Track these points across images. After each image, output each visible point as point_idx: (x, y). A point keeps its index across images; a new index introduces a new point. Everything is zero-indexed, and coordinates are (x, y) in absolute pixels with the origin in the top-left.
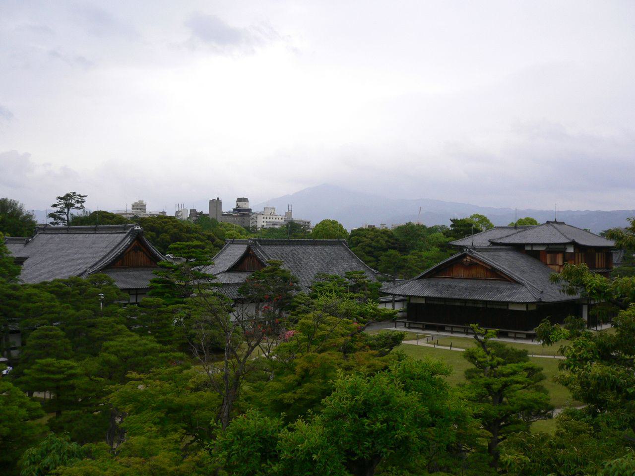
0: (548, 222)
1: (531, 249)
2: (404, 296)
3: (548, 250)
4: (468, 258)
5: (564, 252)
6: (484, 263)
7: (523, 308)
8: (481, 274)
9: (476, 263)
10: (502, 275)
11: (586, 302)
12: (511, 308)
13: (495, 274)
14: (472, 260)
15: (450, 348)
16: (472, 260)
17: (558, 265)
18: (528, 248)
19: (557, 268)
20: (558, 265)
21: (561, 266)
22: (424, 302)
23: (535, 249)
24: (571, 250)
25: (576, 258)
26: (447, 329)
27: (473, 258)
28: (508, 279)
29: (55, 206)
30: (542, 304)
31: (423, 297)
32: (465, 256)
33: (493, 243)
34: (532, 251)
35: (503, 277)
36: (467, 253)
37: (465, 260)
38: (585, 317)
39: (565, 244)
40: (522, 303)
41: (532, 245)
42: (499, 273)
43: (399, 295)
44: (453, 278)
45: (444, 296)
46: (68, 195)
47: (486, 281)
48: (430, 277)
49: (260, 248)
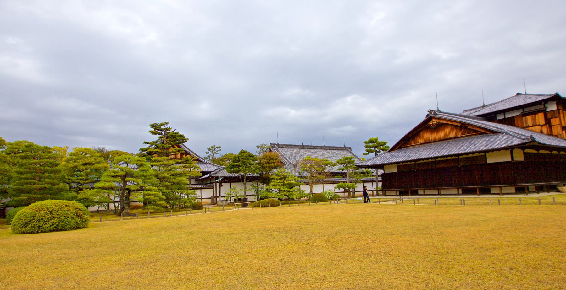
0: (518, 94)
1: (503, 117)
4: (434, 120)
5: (544, 111)
6: (452, 121)
7: (507, 158)
8: (449, 133)
9: (443, 124)
12: (490, 161)
14: (438, 121)
16: (438, 121)
17: (539, 125)
19: (538, 128)
20: (539, 125)
21: (542, 126)
22: (395, 170)
23: (508, 116)
24: (552, 107)
25: (561, 115)
27: (439, 119)
29: (207, 153)
30: (537, 144)
34: (505, 119)
35: (476, 131)
37: (431, 123)
42: (470, 127)
44: (421, 144)
45: (411, 159)
46: (212, 147)
47: (456, 139)
48: (400, 148)
49: (277, 149)
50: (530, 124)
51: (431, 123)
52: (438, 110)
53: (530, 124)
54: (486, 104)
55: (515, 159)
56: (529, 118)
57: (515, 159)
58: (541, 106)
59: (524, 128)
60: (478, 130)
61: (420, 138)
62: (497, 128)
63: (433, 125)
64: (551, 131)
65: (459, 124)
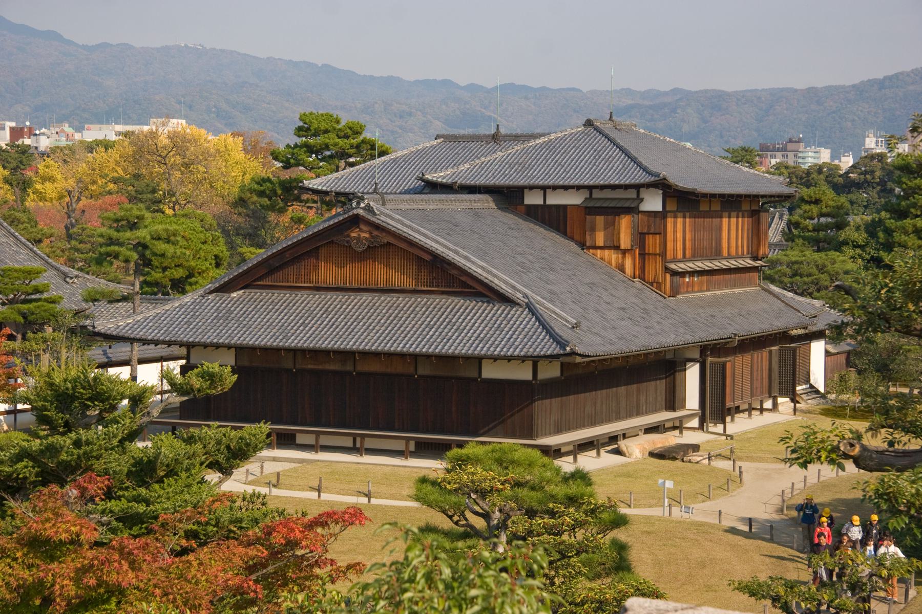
1: (541, 202)
2: (170, 344)
3: (591, 204)
4: (363, 227)
5: (632, 210)
7: (524, 373)
10: (463, 279)
11: (697, 355)
12: (490, 372)
13: (445, 277)
15: (317, 493)
16: (375, 233)
17: (617, 248)
18: (533, 199)
19: (613, 257)
21: (624, 252)
23: (554, 199)
24: (653, 203)
26: (300, 439)
27: (377, 227)
28: (480, 289)
30: (578, 360)
31: (229, 347)
32: (355, 221)
33: (433, 187)
34: (545, 206)
35: (464, 285)
36: (361, 212)
37: (353, 235)
38: (692, 400)
39: (638, 187)
40: (523, 359)
41: (544, 188)
43: (157, 343)
44: (318, 289)
45: (293, 342)
50: (600, 241)
51: (353, 235)
52: (375, 191)
53: (600, 241)
54: (503, 131)
55: (542, 376)
56: (600, 220)
57: (542, 376)
58: (632, 194)
59: (582, 245)
60: (470, 282)
61: (316, 267)
62: (514, 287)
63: (358, 239)
64: (643, 269)
65: (427, 257)
